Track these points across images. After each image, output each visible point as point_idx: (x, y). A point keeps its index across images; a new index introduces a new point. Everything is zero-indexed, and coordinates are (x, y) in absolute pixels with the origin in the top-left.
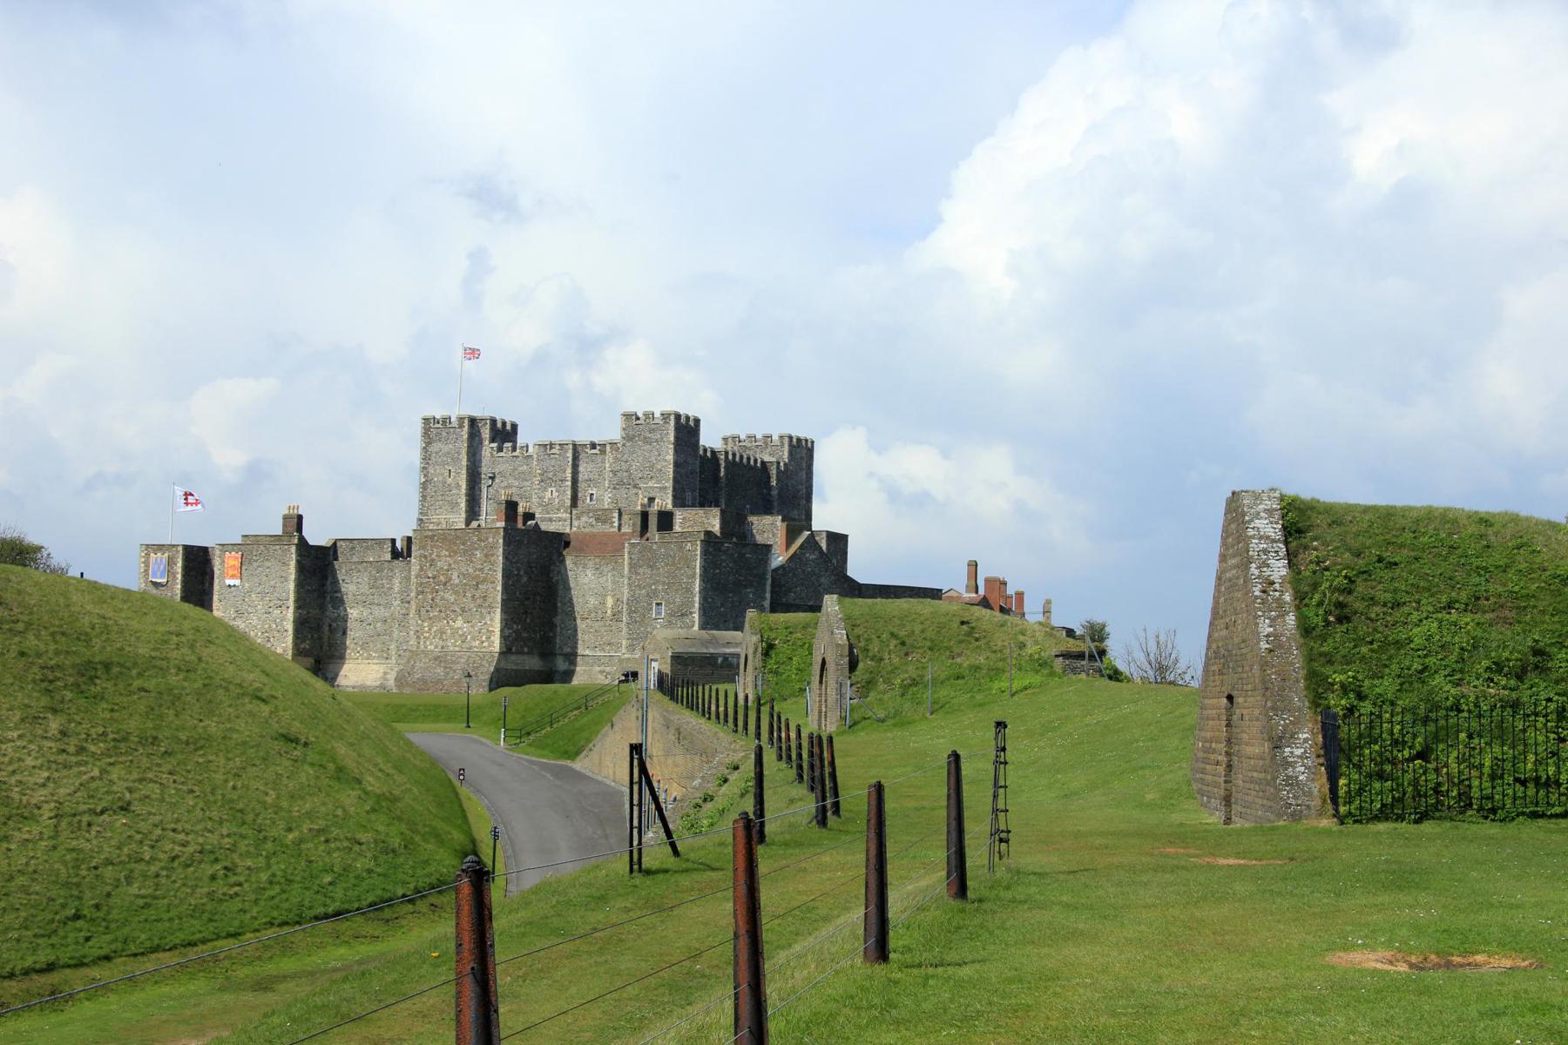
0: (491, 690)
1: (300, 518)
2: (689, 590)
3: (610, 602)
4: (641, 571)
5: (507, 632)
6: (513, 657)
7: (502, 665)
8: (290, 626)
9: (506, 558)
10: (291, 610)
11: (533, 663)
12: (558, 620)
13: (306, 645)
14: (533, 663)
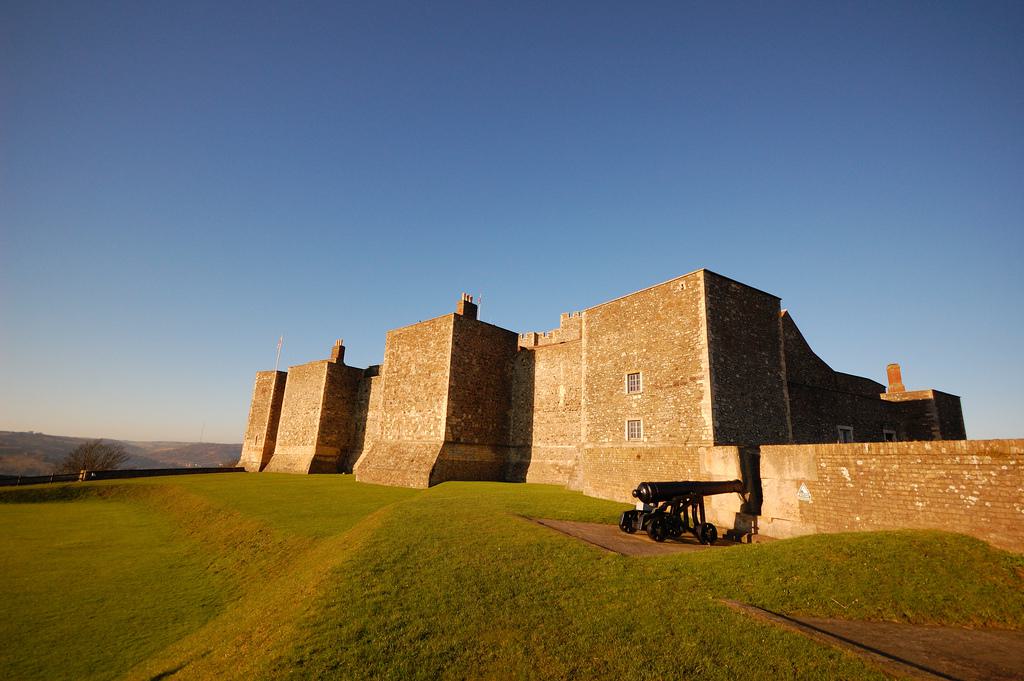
0: (431, 485)
1: (344, 348)
2: (687, 346)
3: (562, 391)
4: (605, 339)
5: (455, 421)
6: (462, 448)
7: (449, 456)
8: (317, 423)
9: (456, 343)
10: (320, 410)
11: (485, 455)
12: (511, 413)
13: (333, 438)
14: (485, 455)
